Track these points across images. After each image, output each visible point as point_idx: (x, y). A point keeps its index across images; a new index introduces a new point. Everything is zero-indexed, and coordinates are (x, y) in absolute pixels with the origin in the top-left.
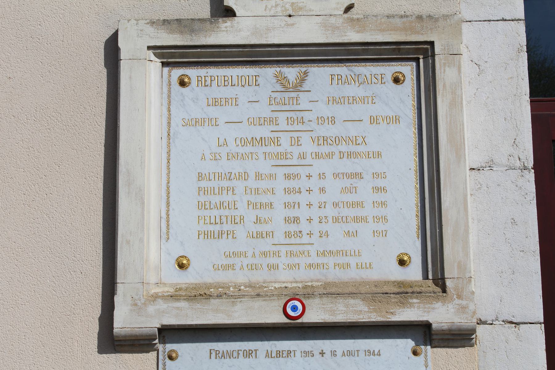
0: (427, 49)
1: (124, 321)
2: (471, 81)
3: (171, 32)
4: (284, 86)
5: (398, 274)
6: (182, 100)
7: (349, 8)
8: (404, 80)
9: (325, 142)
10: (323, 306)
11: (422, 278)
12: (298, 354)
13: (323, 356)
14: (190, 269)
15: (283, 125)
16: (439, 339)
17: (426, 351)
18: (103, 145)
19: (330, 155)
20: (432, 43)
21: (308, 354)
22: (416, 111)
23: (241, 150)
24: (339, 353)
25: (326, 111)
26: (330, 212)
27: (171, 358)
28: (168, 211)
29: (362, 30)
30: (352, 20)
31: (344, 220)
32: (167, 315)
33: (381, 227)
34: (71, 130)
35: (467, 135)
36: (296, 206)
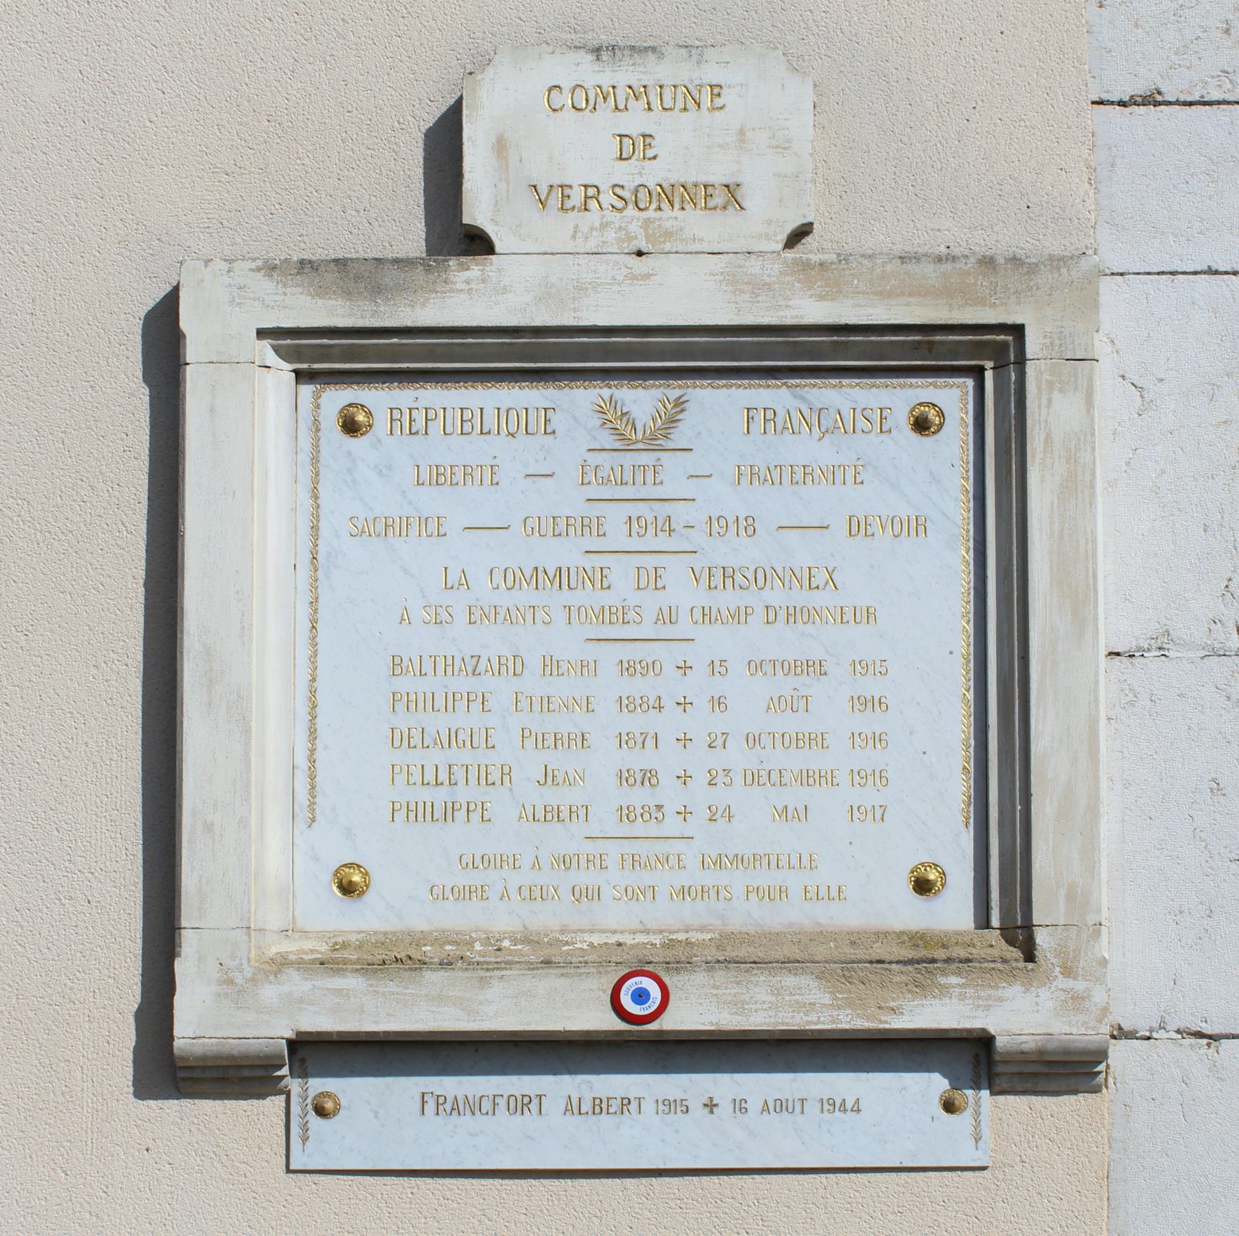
0: (1005, 345)
1: (198, 1023)
2: (1119, 429)
3: (321, 292)
4: (622, 437)
5: (915, 914)
6: (349, 470)
7: (799, 235)
8: (941, 425)
9: (729, 582)
10: (715, 992)
11: (972, 925)
12: (649, 1106)
13: (712, 1112)
14: (370, 896)
15: (617, 537)
16: (1012, 1074)
17: (978, 1103)
18: (142, 582)
19: (740, 615)
20: (1018, 331)
21: (670, 1106)
22: (971, 505)
23: (505, 599)
24: (754, 1105)
25: (733, 503)
26: (738, 757)
27: (321, 1112)
28: (312, 751)
29: (833, 292)
30: (806, 266)
31: (778, 779)
32: (312, 1008)
33: (870, 796)
34: (56, 543)
35: (1104, 566)
36: (650, 743)
